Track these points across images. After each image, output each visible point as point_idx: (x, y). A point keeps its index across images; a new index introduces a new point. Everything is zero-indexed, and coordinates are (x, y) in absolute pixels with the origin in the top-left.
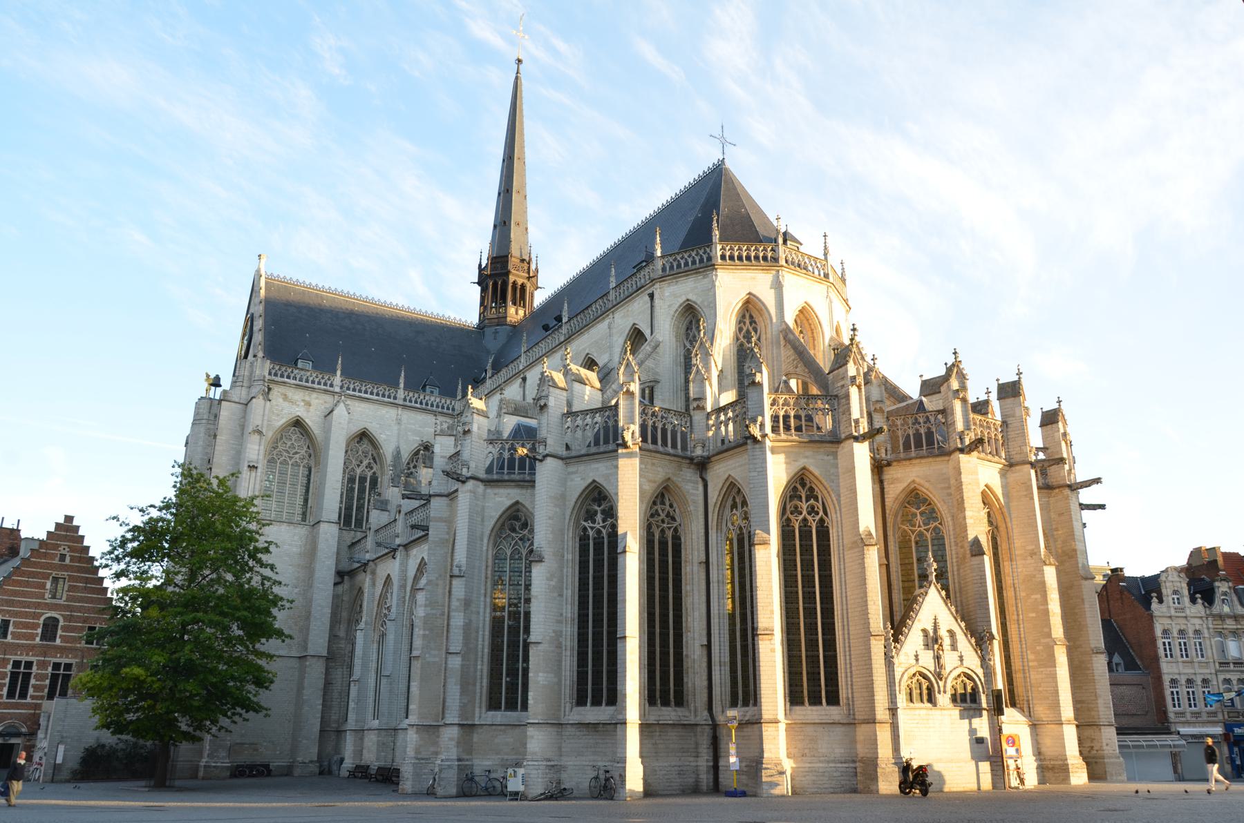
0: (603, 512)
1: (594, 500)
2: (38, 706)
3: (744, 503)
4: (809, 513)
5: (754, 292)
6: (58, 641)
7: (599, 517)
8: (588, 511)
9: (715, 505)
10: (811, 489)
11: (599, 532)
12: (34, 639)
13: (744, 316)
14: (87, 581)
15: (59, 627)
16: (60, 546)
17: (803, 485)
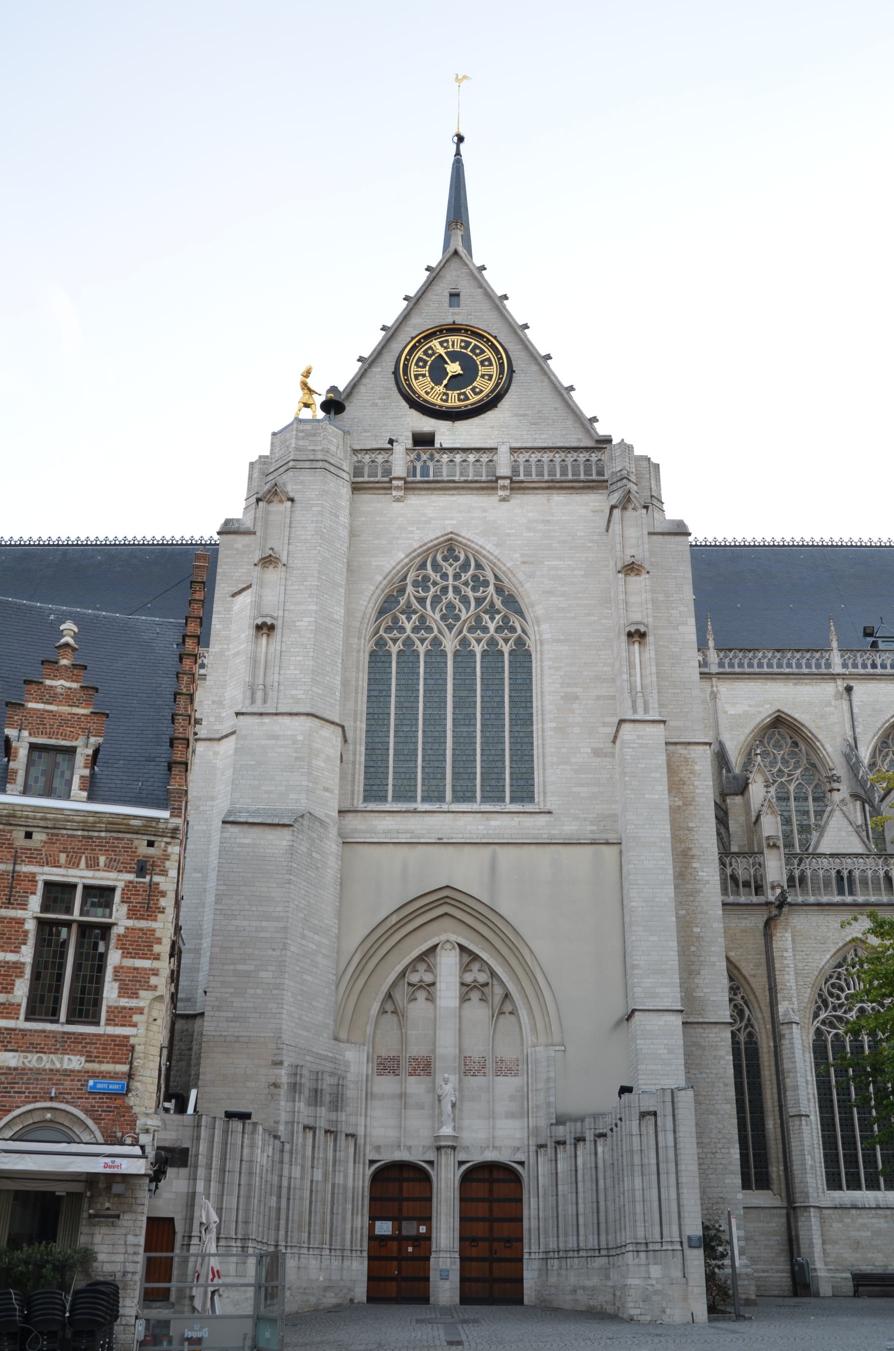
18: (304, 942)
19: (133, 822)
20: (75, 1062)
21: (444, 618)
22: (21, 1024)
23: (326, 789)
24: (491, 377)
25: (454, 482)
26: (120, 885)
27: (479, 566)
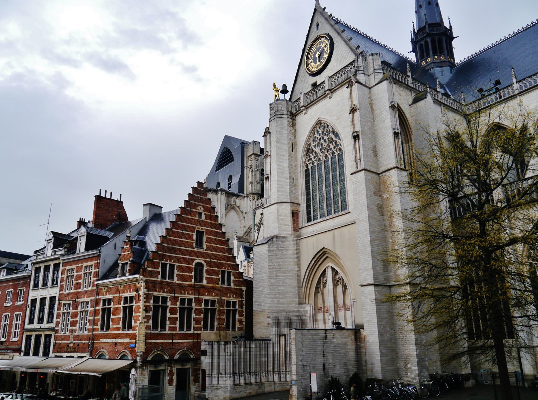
2: (198, 336)
6: (205, 282)
12: (191, 281)
14: (217, 234)
15: (204, 271)
16: (198, 205)
18: (278, 277)
19: (134, 279)
20: (128, 340)
21: (321, 150)
22: (121, 332)
23: (286, 225)
24: (327, 50)
25: (316, 99)
26: (134, 295)
27: (328, 126)
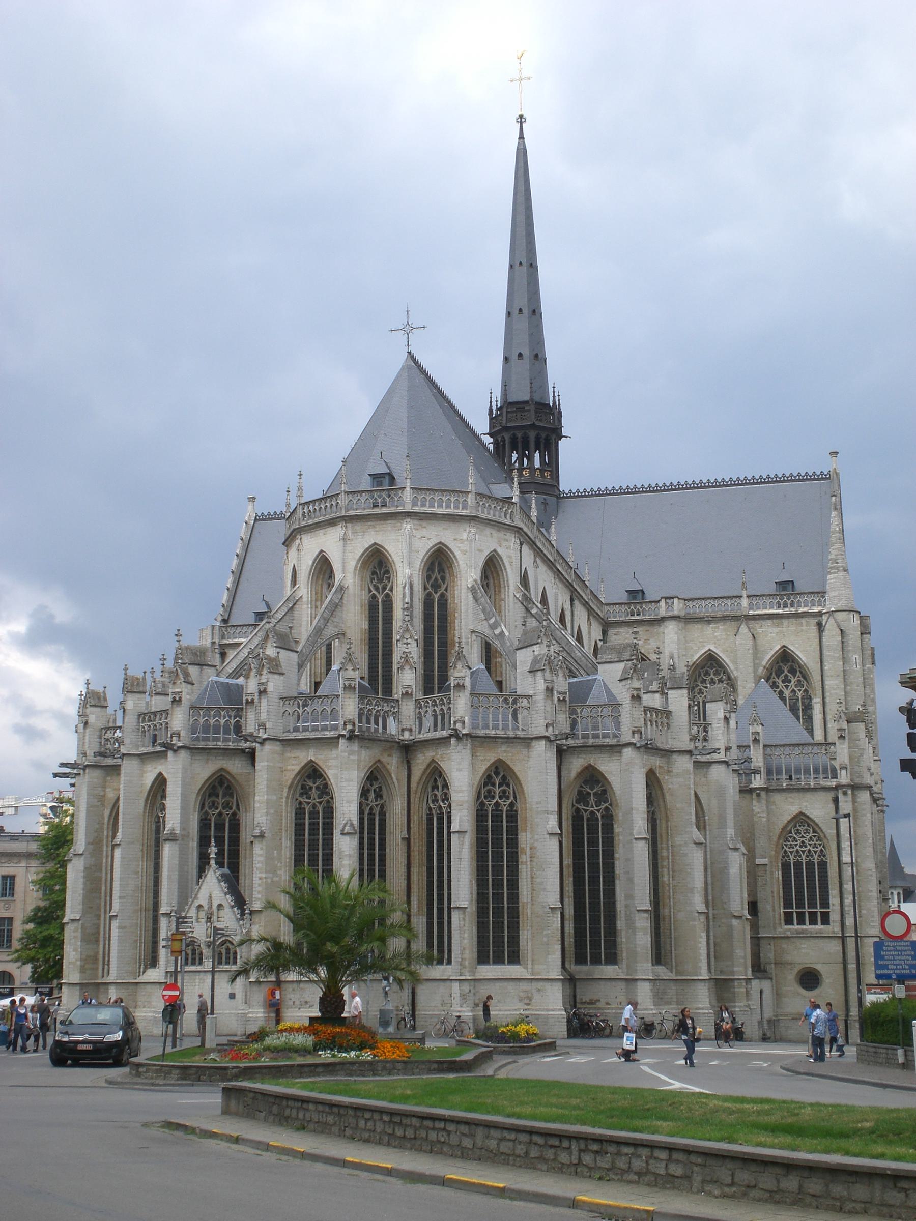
0: (318, 788)
1: (309, 777)
3: (446, 786)
4: (500, 798)
5: (443, 541)
7: (314, 793)
8: (303, 787)
9: (418, 784)
10: (504, 778)
11: (314, 806)
13: (432, 564)
17: (497, 774)
